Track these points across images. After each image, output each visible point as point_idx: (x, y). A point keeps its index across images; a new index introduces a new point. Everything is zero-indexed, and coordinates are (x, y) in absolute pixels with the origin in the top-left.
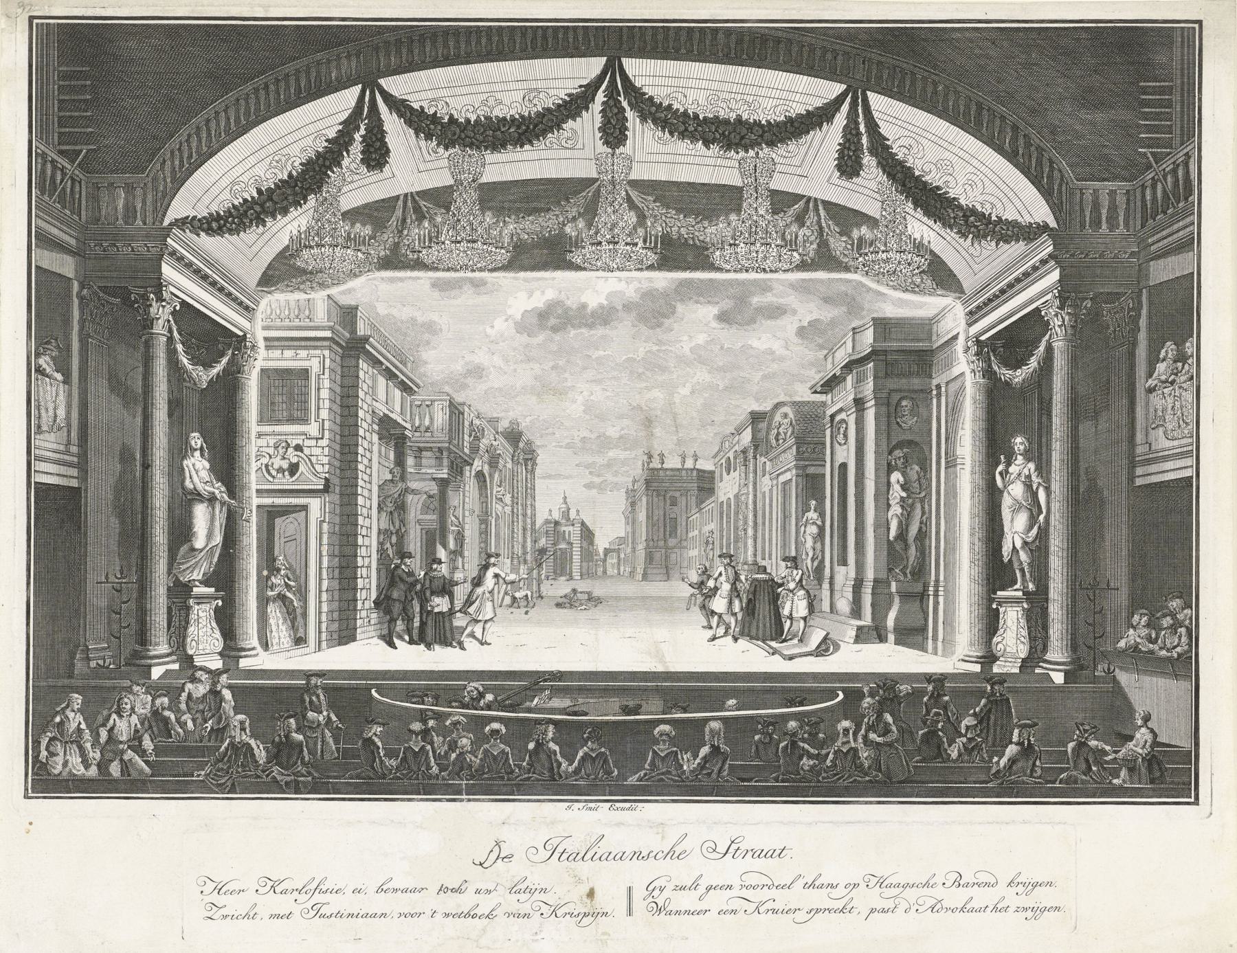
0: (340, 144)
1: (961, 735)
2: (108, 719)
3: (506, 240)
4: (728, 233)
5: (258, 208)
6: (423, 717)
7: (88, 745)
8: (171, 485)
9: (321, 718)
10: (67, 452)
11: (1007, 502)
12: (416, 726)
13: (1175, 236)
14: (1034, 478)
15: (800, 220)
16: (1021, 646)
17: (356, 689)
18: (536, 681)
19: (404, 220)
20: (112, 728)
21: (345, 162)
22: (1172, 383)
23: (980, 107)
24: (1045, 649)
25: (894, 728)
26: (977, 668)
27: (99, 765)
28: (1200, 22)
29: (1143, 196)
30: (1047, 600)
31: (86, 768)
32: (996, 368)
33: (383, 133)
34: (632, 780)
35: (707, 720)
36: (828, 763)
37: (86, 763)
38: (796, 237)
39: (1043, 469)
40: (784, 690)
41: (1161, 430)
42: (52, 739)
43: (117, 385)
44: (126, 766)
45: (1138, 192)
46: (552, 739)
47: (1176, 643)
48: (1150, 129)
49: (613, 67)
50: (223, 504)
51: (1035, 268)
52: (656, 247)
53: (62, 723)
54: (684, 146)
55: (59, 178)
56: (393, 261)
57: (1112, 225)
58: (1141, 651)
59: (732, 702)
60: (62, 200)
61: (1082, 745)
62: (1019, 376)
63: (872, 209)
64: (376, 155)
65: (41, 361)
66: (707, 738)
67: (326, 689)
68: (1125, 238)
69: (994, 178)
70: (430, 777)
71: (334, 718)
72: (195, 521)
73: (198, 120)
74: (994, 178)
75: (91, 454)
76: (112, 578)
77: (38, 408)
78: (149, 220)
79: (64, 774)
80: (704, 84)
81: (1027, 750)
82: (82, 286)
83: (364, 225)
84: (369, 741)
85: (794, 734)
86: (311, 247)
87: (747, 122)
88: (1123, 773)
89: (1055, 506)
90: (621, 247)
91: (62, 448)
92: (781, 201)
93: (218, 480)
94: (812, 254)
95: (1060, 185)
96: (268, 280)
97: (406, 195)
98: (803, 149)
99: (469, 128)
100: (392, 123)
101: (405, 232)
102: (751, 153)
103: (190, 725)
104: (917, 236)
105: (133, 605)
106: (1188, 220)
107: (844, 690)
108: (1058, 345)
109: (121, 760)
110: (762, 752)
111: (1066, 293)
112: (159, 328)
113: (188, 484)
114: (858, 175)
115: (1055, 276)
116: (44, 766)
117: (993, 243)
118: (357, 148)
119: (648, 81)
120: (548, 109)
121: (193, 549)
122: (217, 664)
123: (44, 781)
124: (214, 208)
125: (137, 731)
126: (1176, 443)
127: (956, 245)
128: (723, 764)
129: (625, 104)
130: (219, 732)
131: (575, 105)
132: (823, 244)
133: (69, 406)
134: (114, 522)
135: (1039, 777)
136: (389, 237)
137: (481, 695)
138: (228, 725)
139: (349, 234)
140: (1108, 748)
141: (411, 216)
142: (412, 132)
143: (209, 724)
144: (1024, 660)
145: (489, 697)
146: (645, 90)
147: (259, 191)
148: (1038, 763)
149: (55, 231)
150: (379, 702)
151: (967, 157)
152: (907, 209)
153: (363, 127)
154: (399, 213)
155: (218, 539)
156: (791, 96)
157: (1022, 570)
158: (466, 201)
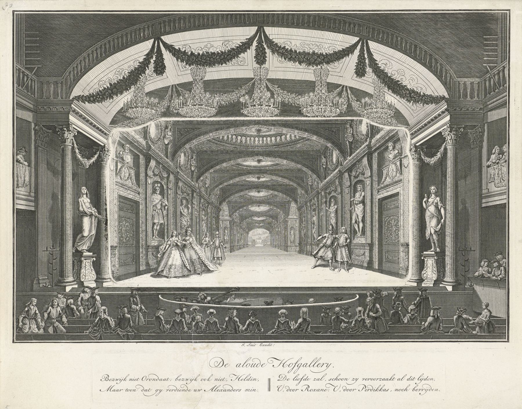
0: (145, 64)
1: (409, 313)
3: (215, 104)
4: (309, 101)
5: (110, 91)
6: (181, 307)
9: (138, 308)
11: (428, 214)
14: (439, 204)
15: (340, 94)
16: (434, 275)
18: (228, 291)
19: (172, 96)
22: (498, 163)
23: (416, 46)
24: (444, 276)
25: (380, 310)
27: (44, 329)
28: (509, 10)
29: (485, 83)
30: (445, 255)
31: (39, 329)
32: (423, 157)
33: (163, 59)
34: (269, 333)
35: (300, 308)
36: (352, 325)
37: (39, 328)
38: (338, 102)
39: (443, 200)
40: (333, 294)
41: (493, 183)
42: (24, 318)
43: (50, 167)
44: (55, 329)
45: (483, 82)
46: (236, 316)
48: (488, 56)
49: (260, 30)
50: (96, 217)
51: (439, 115)
53: (28, 310)
54: (290, 64)
55: (26, 79)
57: (471, 98)
58: (484, 277)
59: (311, 300)
60: (27, 87)
61: (460, 317)
62: (432, 161)
63: (370, 90)
64: (160, 69)
65: (18, 157)
66: (301, 315)
68: (477, 102)
69: (422, 77)
70: (184, 332)
71: (143, 308)
72: (84, 224)
73: (85, 54)
74: (422, 77)
75: (40, 196)
76: (49, 249)
77: (17, 176)
78: (64, 96)
79: (29, 332)
80: (299, 38)
81: (436, 319)
82: (36, 125)
83: (155, 98)
84: (158, 317)
85: (338, 313)
86: (133, 108)
87: (317, 54)
88: (477, 329)
89: (448, 216)
90: (264, 107)
91: (27, 194)
92: (331, 87)
93: (94, 207)
94: (345, 110)
95: (450, 80)
96: (114, 122)
97: (173, 86)
99: (200, 57)
100: (167, 56)
101: (172, 101)
102: (319, 67)
103: (82, 311)
104: (389, 102)
106: (505, 94)
107: (359, 294)
108: (449, 147)
109: (54, 326)
111: (453, 125)
112: (68, 143)
114: (364, 76)
115: (448, 118)
116: (21, 329)
117: (422, 105)
118: (152, 66)
119: (275, 36)
120: (233, 49)
121: (83, 236)
122: (93, 285)
123: (21, 336)
124: (91, 92)
125: (60, 314)
126: (499, 189)
128: (308, 327)
129: (265, 46)
130: (95, 314)
132: (349, 106)
133: (30, 176)
134: (50, 224)
135: (442, 331)
136: (165, 103)
137: (206, 298)
138: (98, 311)
139: (148, 102)
140: (471, 318)
142: (175, 59)
143: (90, 311)
144: (435, 281)
145: (209, 298)
146: (274, 40)
147: (110, 84)
148: (441, 325)
149: (25, 102)
150: (162, 300)
151: (410, 68)
152: (385, 90)
153: (154, 57)
154: (170, 92)
155: (94, 232)
156: (336, 43)
157: (434, 243)
158: (198, 89)
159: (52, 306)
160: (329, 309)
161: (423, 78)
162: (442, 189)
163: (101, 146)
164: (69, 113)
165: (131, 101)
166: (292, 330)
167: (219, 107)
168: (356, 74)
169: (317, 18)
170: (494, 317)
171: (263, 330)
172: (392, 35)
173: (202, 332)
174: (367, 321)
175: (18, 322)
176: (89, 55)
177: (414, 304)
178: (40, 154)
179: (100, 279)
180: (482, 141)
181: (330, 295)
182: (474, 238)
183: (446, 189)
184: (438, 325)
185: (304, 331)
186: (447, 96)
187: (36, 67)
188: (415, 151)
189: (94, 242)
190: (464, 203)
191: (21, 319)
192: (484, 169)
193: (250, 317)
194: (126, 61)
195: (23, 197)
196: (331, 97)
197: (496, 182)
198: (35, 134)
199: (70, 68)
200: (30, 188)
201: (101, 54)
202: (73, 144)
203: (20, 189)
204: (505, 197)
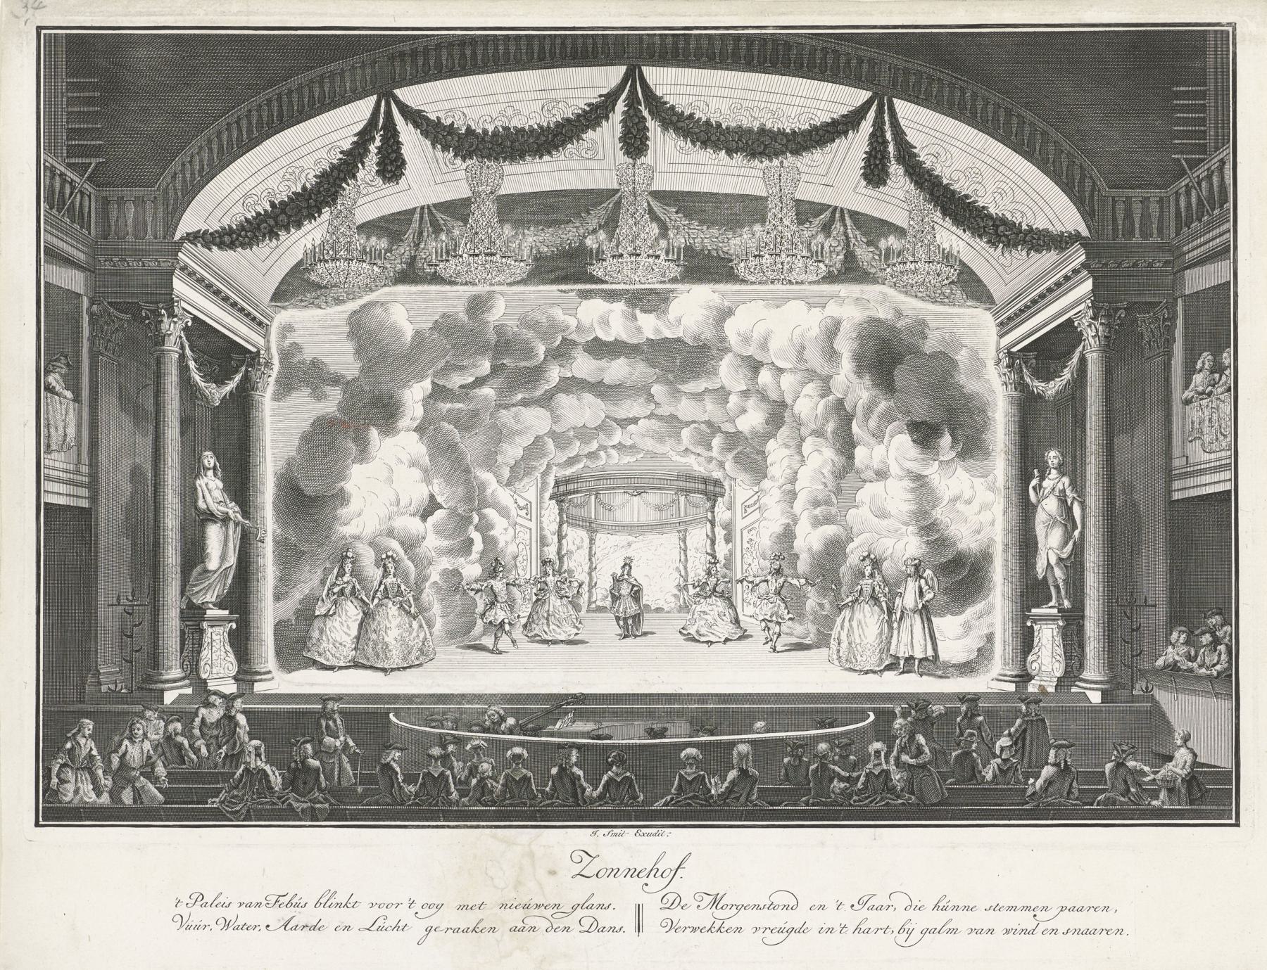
1: (995, 756)
2: (120, 746)
3: (526, 253)
4: (753, 244)
5: (272, 222)
7: (100, 772)
8: (183, 502)
9: (338, 744)
10: (77, 472)
11: (1041, 517)
12: (436, 751)
13: (1211, 244)
14: (1068, 492)
15: (826, 229)
16: (1057, 665)
17: (374, 713)
18: (558, 705)
19: (421, 233)
20: (125, 754)
21: (360, 175)
22: (1210, 394)
23: (1009, 112)
24: (1081, 665)
25: (927, 750)
26: (1011, 687)
27: (110, 793)
29: (1177, 201)
30: (1083, 617)
31: (99, 795)
32: (1028, 380)
34: (658, 805)
35: (733, 744)
36: (860, 785)
37: (98, 791)
38: (822, 248)
39: (1078, 484)
40: (812, 711)
41: (1198, 442)
42: (65, 765)
45: (1172, 199)
46: (576, 764)
47: (1215, 662)
51: (1067, 278)
52: (679, 259)
53: (73, 748)
54: (706, 155)
55: (68, 191)
56: (409, 275)
57: (1145, 234)
58: (1179, 669)
59: (760, 724)
61: (1120, 765)
62: (1051, 389)
63: (900, 219)
64: (392, 167)
65: (51, 379)
66: (735, 761)
67: (343, 713)
68: (1160, 247)
69: (1024, 186)
70: (450, 803)
71: (351, 743)
72: (208, 542)
73: (211, 131)
76: (123, 601)
79: (76, 801)
80: (726, 92)
81: (1064, 770)
82: (92, 303)
83: (379, 238)
85: (825, 757)
86: (326, 261)
87: (770, 131)
88: (1163, 794)
89: (1091, 521)
90: (643, 259)
91: (72, 467)
92: (806, 211)
93: (232, 500)
94: (838, 265)
96: (280, 295)
97: (423, 208)
98: (830, 157)
100: (408, 135)
101: (422, 245)
102: (776, 162)
103: (204, 750)
104: (946, 246)
105: (146, 625)
107: (874, 710)
109: (134, 787)
110: (792, 775)
111: (1100, 302)
112: (171, 345)
113: (201, 505)
114: (885, 184)
115: (1088, 285)
116: (56, 792)
117: (1024, 253)
118: (372, 160)
119: (672, 90)
120: (568, 120)
121: (206, 571)
122: (230, 688)
123: (53, 811)
124: (226, 222)
125: (149, 757)
126: (1213, 456)
127: (987, 255)
128: (752, 789)
129: (646, 113)
130: (234, 758)
131: (595, 115)
132: (850, 256)
134: (126, 542)
135: (1077, 799)
136: (404, 250)
137: (503, 719)
138: (242, 751)
139: (364, 250)
140: (1146, 769)
141: (428, 229)
142: (428, 143)
143: (224, 750)
145: (511, 721)
146: (667, 99)
147: (273, 204)
148: (1075, 784)
150: (397, 726)
152: (936, 219)
153: (378, 139)
154: (415, 225)
155: (232, 560)
156: (815, 104)
157: (1057, 587)
158: (485, 213)
159: (131, 739)
160: (801, 746)
161: (1026, 188)
162: (1074, 457)
163: (250, 352)
164: (170, 274)
165: (323, 244)
166: (712, 797)
167: (536, 259)
168: (865, 179)
169: (770, 45)
170: (1203, 765)
171: (642, 797)
172: (952, 86)
173: (494, 803)
174: (897, 776)
175: (48, 777)
176: (219, 133)
177: (1010, 735)
178: (102, 373)
179: (246, 675)
180: (1170, 341)
181: (802, 712)
182: (1154, 580)
183: (1084, 456)
184: (1067, 785)
185: (742, 799)
186: (1085, 232)
187: (94, 161)
188: (1008, 366)
189: (232, 586)
190: (1129, 489)
191: (55, 769)
192: (1177, 407)
193: (610, 766)
194: (311, 147)
195: (61, 474)
196: (807, 234)
197: (1207, 438)
198: (92, 322)
199: (175, 166)
200: (79, 455)
201: (250, 131)
202: (182, 347)
203: (54, 455)
204: (1228, 475)
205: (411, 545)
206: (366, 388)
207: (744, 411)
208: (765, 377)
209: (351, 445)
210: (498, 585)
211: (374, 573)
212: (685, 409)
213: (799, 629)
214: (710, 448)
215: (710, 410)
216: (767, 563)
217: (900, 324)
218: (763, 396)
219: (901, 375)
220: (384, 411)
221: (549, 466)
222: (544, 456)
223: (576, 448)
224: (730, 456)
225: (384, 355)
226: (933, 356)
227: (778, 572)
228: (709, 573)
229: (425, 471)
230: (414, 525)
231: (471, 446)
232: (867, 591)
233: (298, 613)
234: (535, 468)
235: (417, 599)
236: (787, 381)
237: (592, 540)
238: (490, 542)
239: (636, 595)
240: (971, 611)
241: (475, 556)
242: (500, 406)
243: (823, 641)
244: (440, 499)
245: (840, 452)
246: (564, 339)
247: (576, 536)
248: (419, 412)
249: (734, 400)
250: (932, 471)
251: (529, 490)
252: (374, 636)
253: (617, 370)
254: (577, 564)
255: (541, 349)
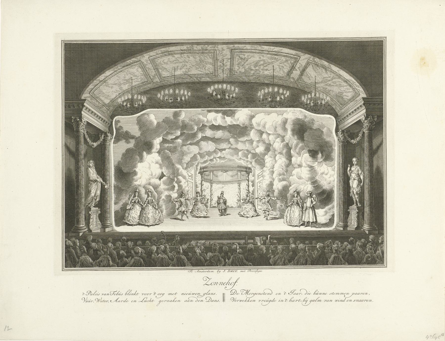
205: (156, 187)
206: (142, 140)
207: (258, 147)
208: (264, 136)
209: (138, 157)
210: (183, 200)
211: (145, 196)
212: (240, 146)
213: (275, 213)
214: (247, 158)
215: (247, 146)
216: (265, 193)
217: (306, 120)
218: (264, 143)
219: (306, 135)
220: (148, 147)
221: (198, 163)
222: (197, 160)
223: (207, 158)
224: (254, 160)
225: (148, 130)
226: (316, 130)
227: (268, 196)
228: (247, 196)
229: (160, 165)
230: (157, 181)
231: (174, 157)
232: (296, 201)
233: (121, 208)
234: (193, 164)
235: (158, 204)
236: (271, 137)
237: (211, 186)
238: (180, 186)
239: (225, 203)
240: (327, 208)
241: (175, 191)
242: (183, 145)
243: (282, 217)
244: (165, 174)
245: (287, 159)
246: (203, 125)
247: (206, 185)
248: (158, 147)
249: (255, 143)
250: (315, 165)
251: (192, 171)
252: (145, 215)
253: (219, 134)
254: (207, 193)
255: (196, 128)
